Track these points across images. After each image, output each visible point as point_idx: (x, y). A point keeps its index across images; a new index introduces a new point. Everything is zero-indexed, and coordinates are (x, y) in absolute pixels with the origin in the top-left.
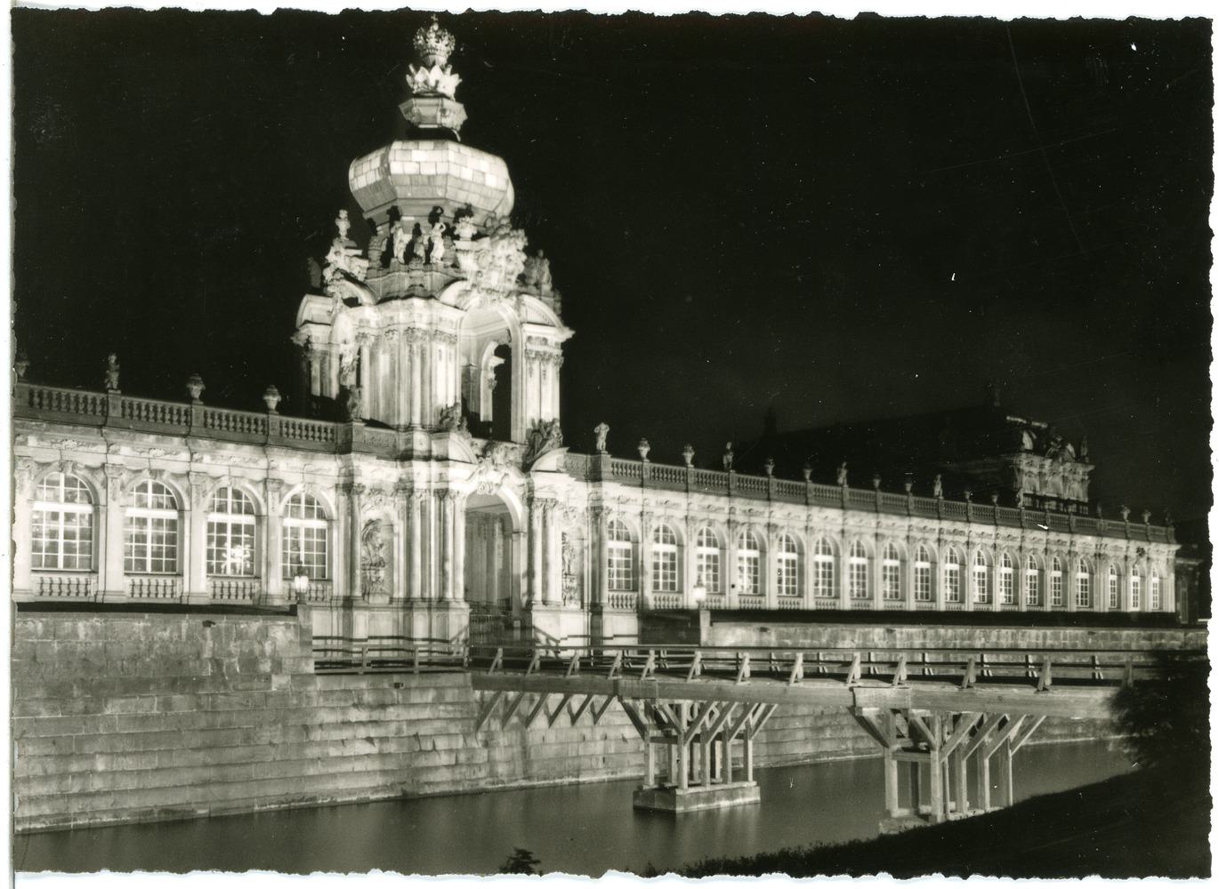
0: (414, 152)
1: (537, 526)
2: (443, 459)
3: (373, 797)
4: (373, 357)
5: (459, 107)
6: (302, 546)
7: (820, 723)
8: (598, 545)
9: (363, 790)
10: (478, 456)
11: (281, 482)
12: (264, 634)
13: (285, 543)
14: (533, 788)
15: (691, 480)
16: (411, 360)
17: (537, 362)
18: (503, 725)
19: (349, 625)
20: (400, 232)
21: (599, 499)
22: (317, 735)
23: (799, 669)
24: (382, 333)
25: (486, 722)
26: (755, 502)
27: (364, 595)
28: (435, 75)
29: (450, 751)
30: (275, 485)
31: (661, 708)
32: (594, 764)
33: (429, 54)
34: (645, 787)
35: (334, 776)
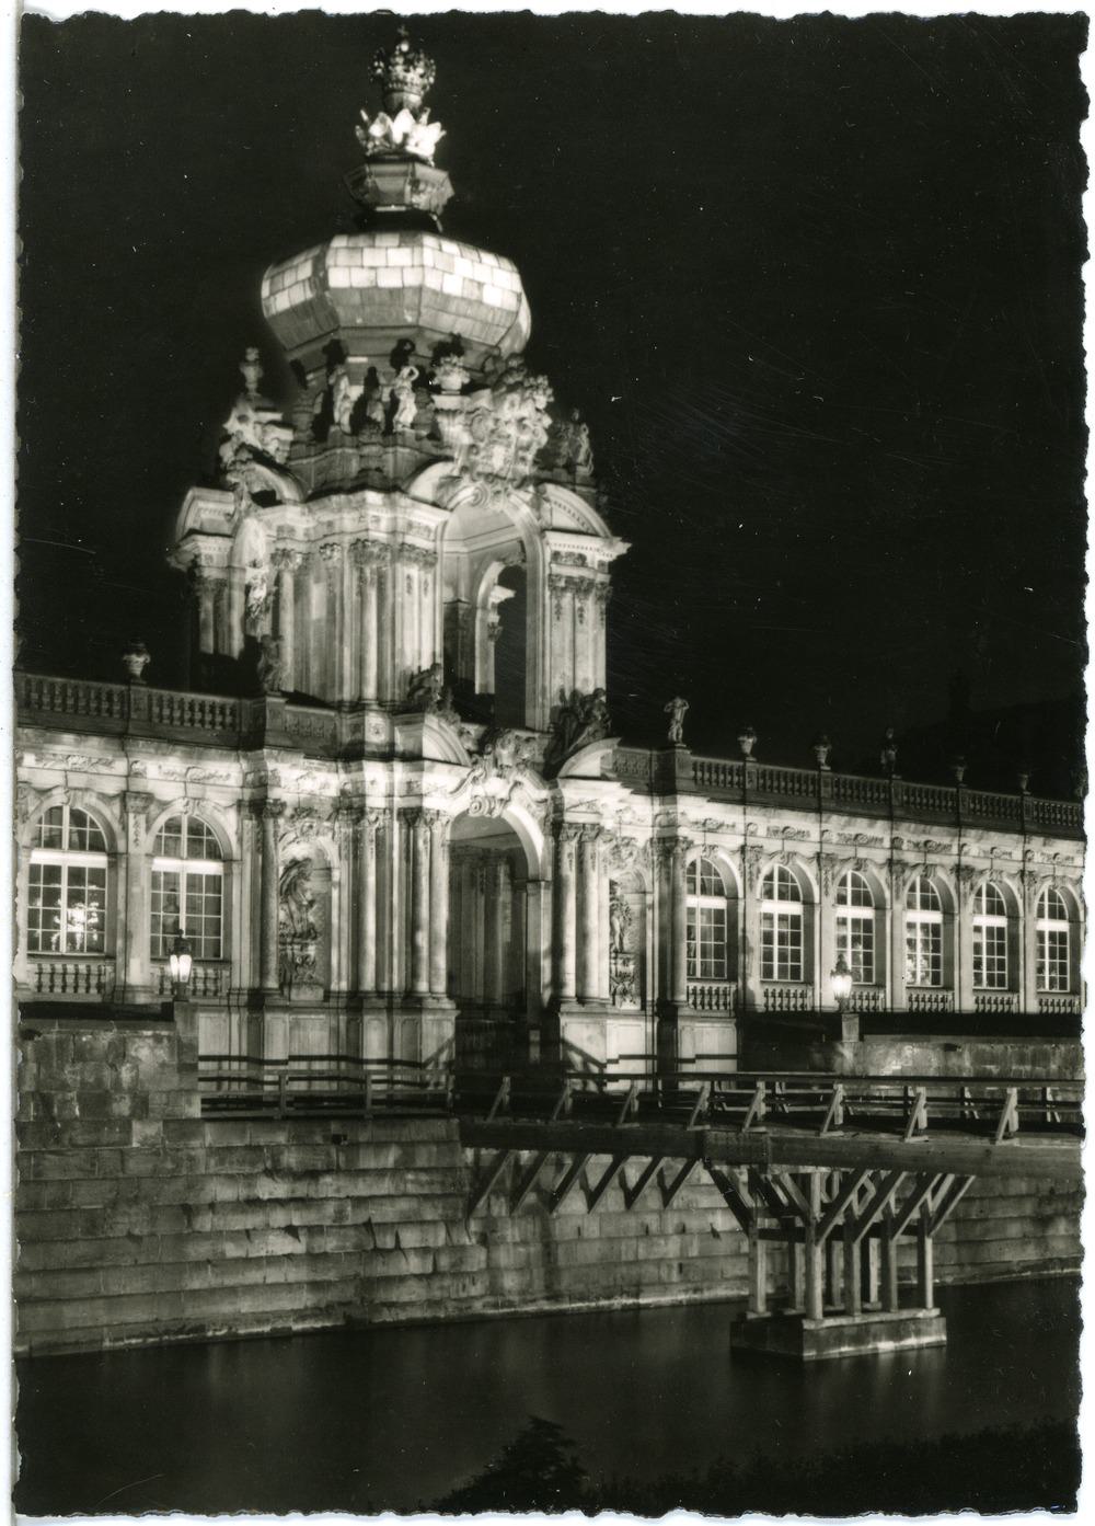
0: (367, 252)
1: (569, 872)
2: (414, 758)
3: (297, 1327)
4: (300, 591)
5: (441, 176)
6: (183, 904)
7: (1049, 1210)
8: (670, 902)
9: (279, 1315)
10: (470, 753)
11: (149, 798)
12: (119, 1053)
13: (155, 898)
14: (562, 1313)
15: (826, 792)
16: (362, 593)
17: (569, 595)
18: (512, 1209)
19: (257, 1037)
20: (344, 383)
21: (673, 825)
22: (205, 1223)
23: (1011, 1116)
24: (315, 548)
25: (482, 1202)
26: (936, 829)
27: (281, 986)
28: (401, 125)
29: (424, 1251)
30: (139, 803)
31: (777, 1180)
32: (664, 1273)
33: (394, 90)
34: (751, 1316)
35: (232, 1291)
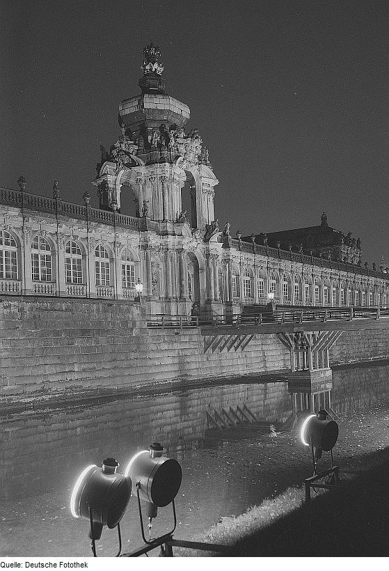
28: (156, 66)
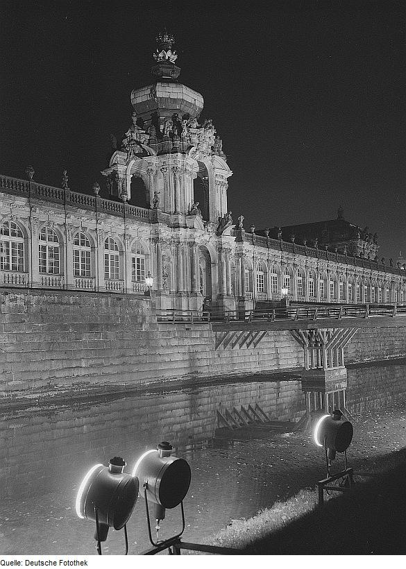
1: (223, 260)
